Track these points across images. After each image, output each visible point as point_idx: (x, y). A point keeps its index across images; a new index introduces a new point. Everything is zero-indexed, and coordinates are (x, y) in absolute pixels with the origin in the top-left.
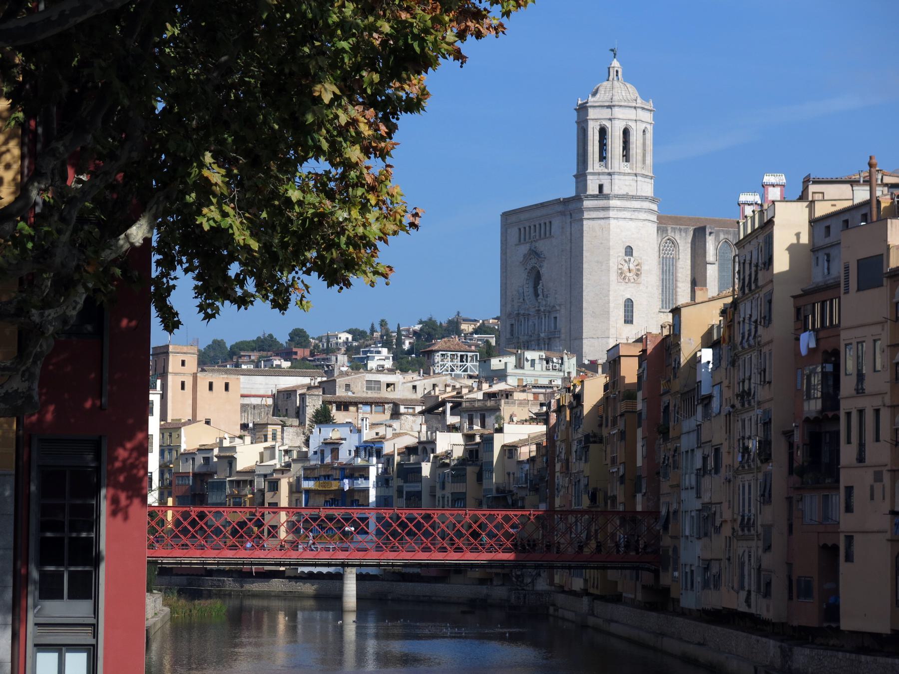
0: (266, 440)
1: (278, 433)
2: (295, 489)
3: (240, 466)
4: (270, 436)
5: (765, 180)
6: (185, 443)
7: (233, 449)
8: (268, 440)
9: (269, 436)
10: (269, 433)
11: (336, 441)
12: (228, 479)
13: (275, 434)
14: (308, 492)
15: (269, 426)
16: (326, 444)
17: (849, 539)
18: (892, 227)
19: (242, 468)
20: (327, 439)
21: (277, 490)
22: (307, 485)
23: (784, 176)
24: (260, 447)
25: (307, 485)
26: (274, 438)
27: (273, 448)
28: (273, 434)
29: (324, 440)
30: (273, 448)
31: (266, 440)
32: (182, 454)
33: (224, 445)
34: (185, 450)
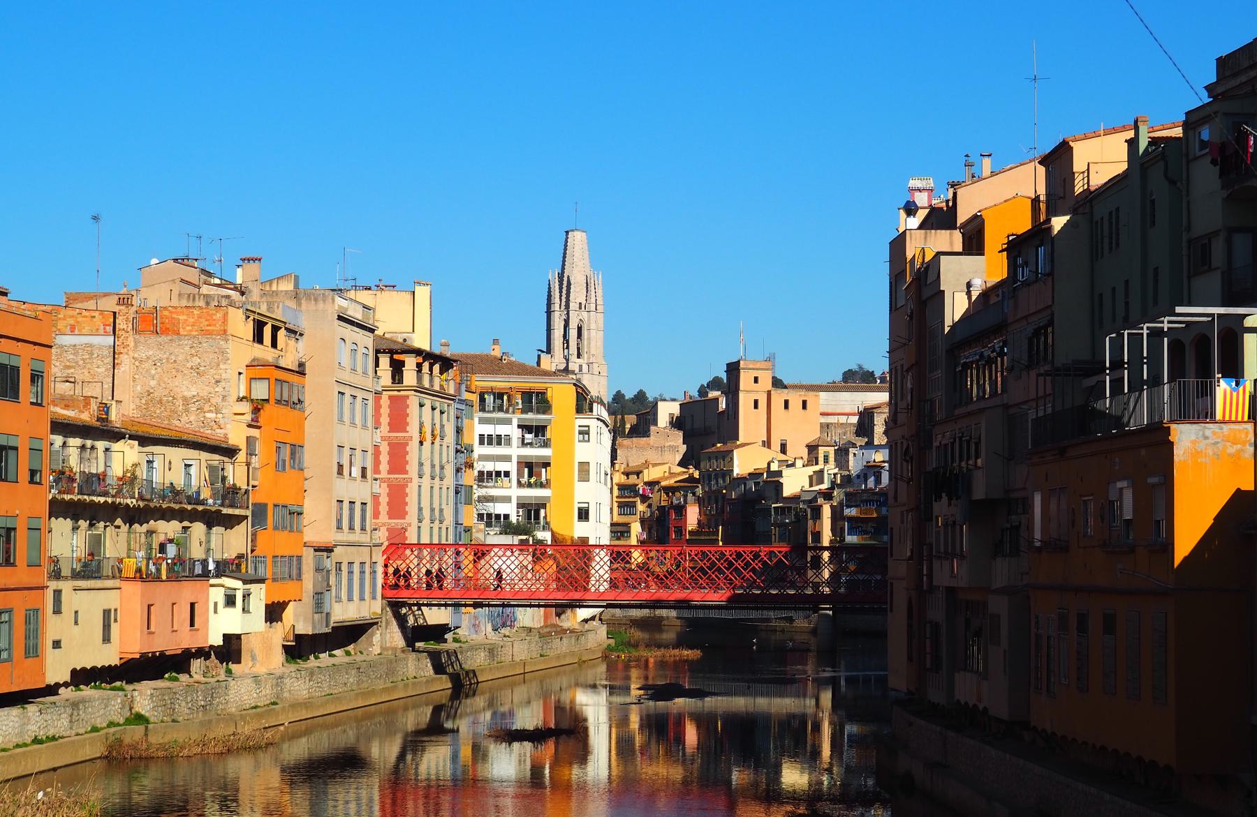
0: (817, 464)
1: (830, 456)
2: (837, 516)
3: (787, 492)
4: (821, 459)
5: (910, 185)
6: (738, 466)
7: (779, 473)
8: (819, 463)
9: (820, 459)
10: (820, 455)
11: (879, 464)
12: (773, 506)
13: (827, 456)
14: (851, 519)
15: (820, 448)
16: (868, 467)
17: (892, 584)
18: (911, 239)
19: (789, 494)
20: (869, 462)
21: (820, 518)
22: (851, 512)
23: (931, 180)
24: (811, 470)
25: (851, 512)
26: (826, 460)
27: (822, 471)
28: (824, 456)
29: (867, 462)
30: (822, 471)
31: (817, 464)
32: (734, 479)
33: (772, 469)
34: (738, 474)
